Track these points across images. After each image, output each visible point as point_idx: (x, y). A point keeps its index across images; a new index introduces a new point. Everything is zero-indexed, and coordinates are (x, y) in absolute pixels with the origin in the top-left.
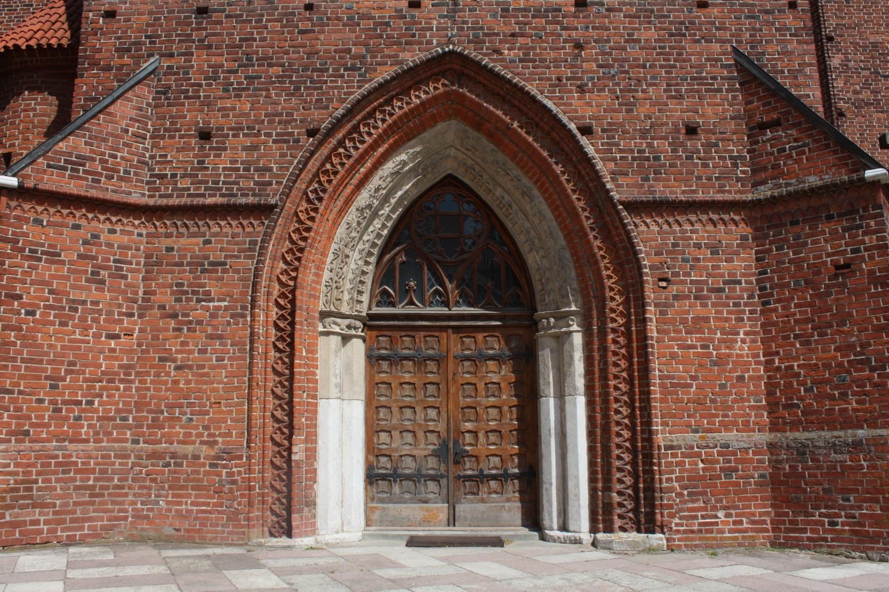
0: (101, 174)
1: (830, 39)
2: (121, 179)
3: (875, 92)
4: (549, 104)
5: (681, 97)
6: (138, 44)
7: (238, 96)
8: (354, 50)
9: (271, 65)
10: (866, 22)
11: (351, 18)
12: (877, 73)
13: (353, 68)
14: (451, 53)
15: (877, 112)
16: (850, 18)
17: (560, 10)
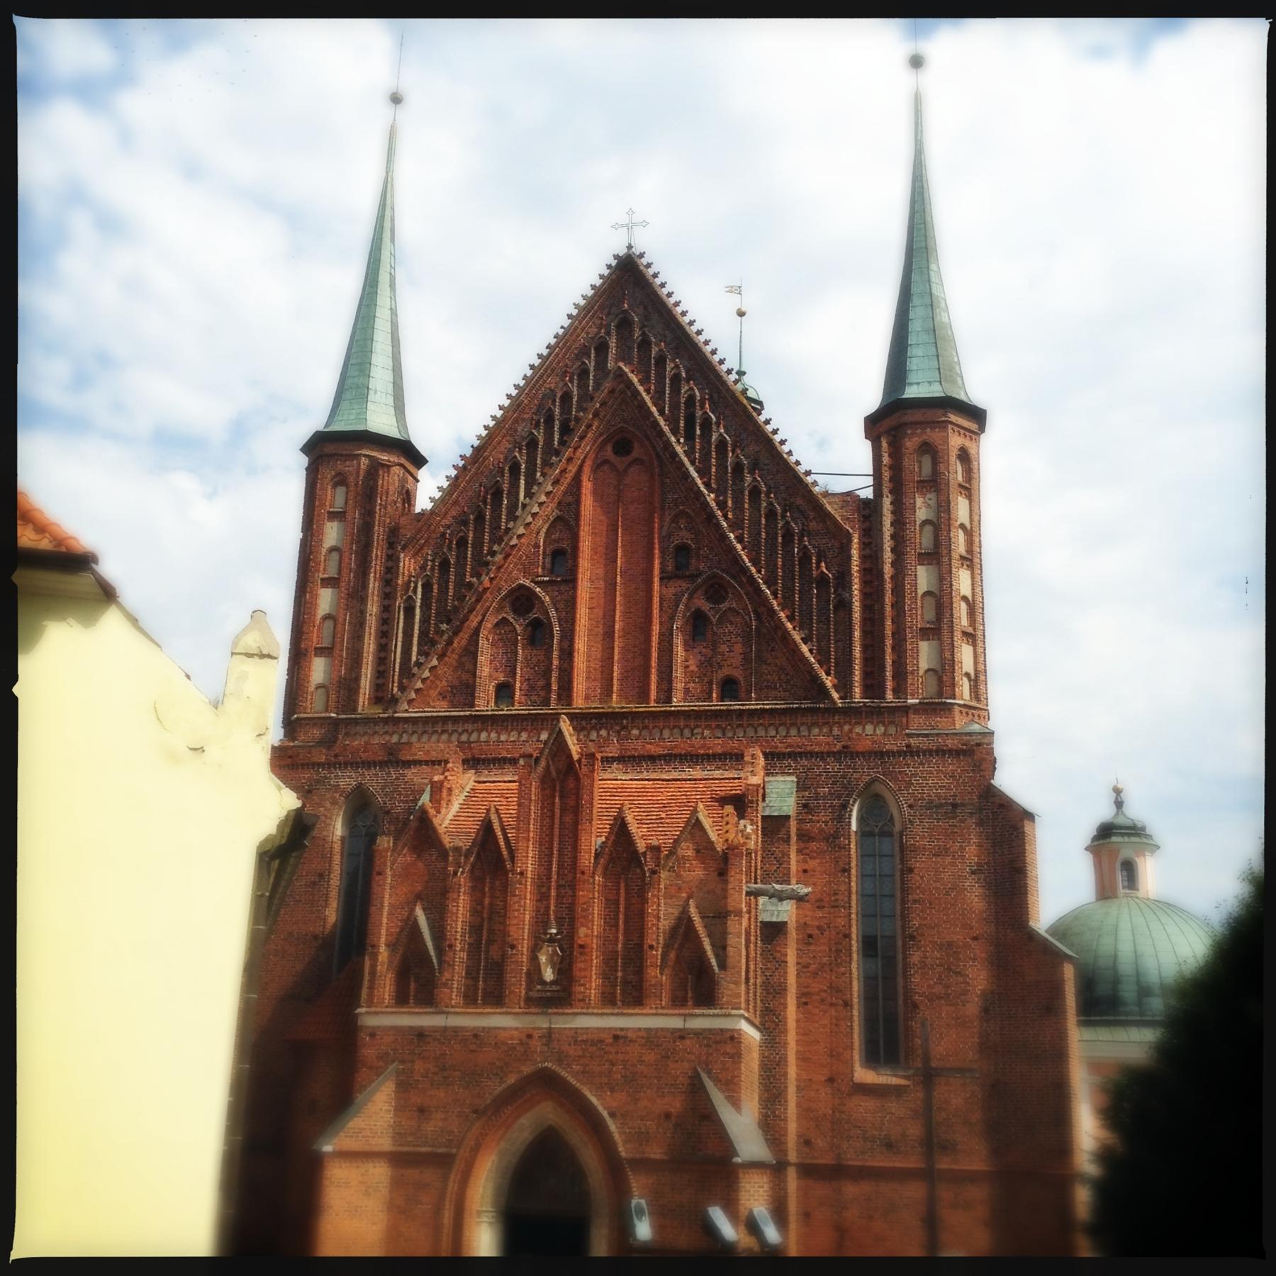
0: (369, 1137)
1: (912, 937)
2: (379, 1137)
3: (947, 987)
4: (594, 1100)
5: (664, 1096)
6: (387, 1054)
7: (438, 1088)
8: (497, 1063)
9: (455, 1070)
10: (945, 922)
11: (496, 1044)
12: (949, 969)
13: (497, 1074)
14: (546, 1067)
15: (947, 1005)
16: (931, 919)
17: (603, 1041)
